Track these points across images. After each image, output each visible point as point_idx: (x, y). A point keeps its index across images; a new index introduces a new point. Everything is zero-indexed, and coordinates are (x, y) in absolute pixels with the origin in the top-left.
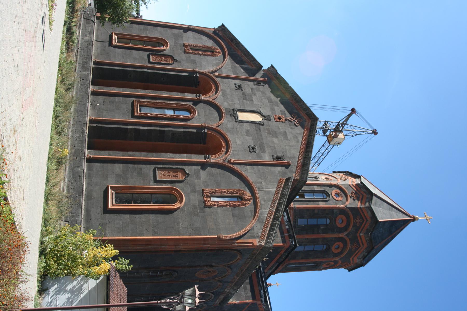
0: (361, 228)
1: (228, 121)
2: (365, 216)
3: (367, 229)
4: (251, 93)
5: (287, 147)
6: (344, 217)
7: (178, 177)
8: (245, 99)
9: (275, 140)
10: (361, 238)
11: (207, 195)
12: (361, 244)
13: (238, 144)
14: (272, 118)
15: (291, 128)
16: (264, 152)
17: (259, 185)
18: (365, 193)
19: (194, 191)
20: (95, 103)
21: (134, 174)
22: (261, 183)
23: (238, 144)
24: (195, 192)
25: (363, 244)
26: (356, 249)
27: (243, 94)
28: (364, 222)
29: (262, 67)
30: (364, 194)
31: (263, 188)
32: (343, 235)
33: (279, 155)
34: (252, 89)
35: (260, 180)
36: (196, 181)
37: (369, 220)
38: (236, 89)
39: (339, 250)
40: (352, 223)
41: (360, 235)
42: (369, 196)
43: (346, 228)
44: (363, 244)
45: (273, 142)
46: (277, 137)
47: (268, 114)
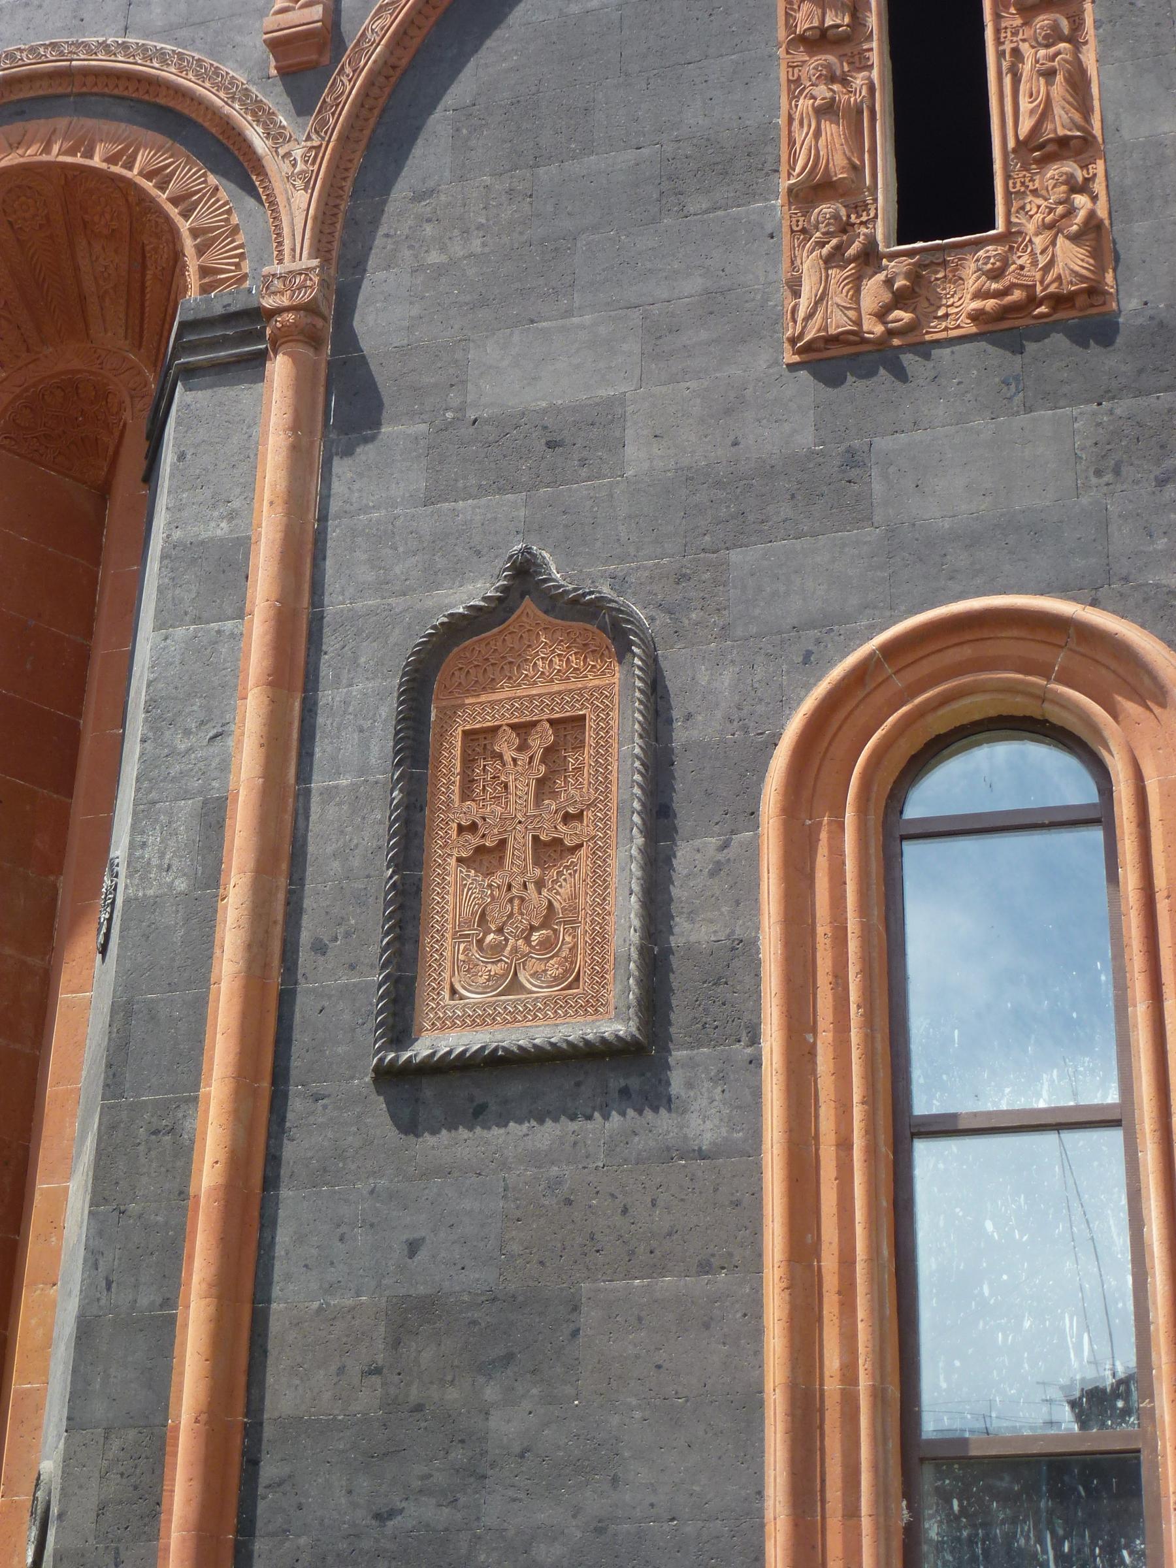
7: (569, 728)
11: (900, 299)
19: (834, 485)
21: (507, 1426)
24: (853, 460)
36: (638, 456)
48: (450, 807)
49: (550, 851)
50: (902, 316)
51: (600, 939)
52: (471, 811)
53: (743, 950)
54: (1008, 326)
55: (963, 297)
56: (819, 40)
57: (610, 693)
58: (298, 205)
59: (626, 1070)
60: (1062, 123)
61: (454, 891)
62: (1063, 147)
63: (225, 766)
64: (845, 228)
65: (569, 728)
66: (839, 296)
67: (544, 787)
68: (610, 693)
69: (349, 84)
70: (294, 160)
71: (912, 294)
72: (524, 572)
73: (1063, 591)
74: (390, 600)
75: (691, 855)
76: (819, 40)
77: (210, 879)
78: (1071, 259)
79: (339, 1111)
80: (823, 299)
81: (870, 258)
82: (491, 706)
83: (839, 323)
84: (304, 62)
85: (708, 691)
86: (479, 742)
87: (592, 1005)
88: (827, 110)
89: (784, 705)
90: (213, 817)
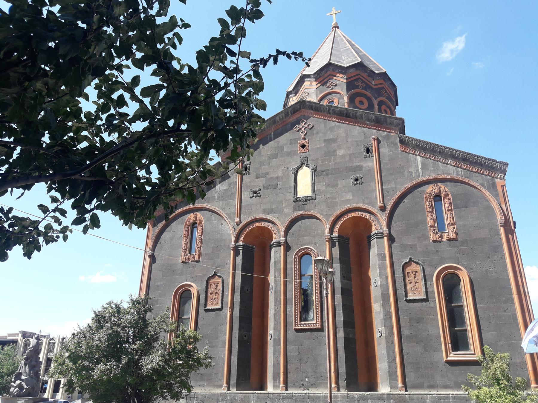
0: (368, 83)
1: (315, 208)
2: (354, 76)
3: (369, 76)
4: (264, 178)
5: (349, 140)
6: (358, 99)
7: (416, 272)
8: (276, 186)
9: (340, 153)
10: (376, 85)
12: (382, 86)
13: (351, 198)
14: (304, 156)
15: (317, 133)
16: (359, 168)
17: (414, 175)
18: (327, 72)
20: (305, 383)
21: (420, 327)
22: (411, 173)
23: (351, 198)
25: (381, 84)
26: (386, 92)
27: (267, 188)
28: (361, 77)
29: (219, 162)
30: (329, 73)
31: (418, 171)
32: (376, 103)
33: (363, 150)
34: (257, 177)
35: (406, 173)
37: (358, 72)
38: (260, 197)
39: (388, 110)
40: (363, 91)
41: (375, 85)
42: (331, 68)
43: (369, 100)
44: (381, 84)
45: (343, 156)
46: (335, 151)
47: (299, 161)
48: (407, 279)
49: (416, 282)
50: (440, 239)
51: (421, 290)
52: (409, 279)
53: (433, 291)
54: (449, 240)
55: (445, 237)
56: (430, 212)
57: (419, 268)
58: (384, 224)
59: (426, 300)
60: (452, 222)
61: (409, 286)
62: (452, 224)
63: (387, 274)
64: (434, 230)
65: (416, 272)
66: (435, 236)
67: (415, 277)
68: (419, 268)
69: (387, 211)
70: (383, 218)
71: (441, 237)
72: (411, 259)
73: (456, 263)
74: (401, 260)
75: (428, 284)
76: (430, 212)
77: (387, 283)
78: (454, 235)
79: (402, 303)
80: (432, 237)
81: (437, 233)
82: (408, 269)
83: (435, 239)
84: (383, 209)
85: (428, 270)
86: (408, 273)
87: (421, 295)
88: (431, 219)
89: (434, 272)
90: (387, 278)
